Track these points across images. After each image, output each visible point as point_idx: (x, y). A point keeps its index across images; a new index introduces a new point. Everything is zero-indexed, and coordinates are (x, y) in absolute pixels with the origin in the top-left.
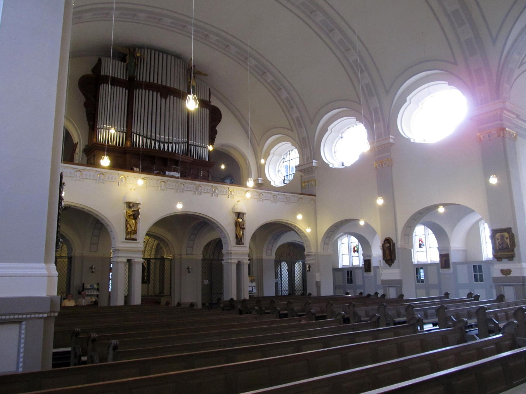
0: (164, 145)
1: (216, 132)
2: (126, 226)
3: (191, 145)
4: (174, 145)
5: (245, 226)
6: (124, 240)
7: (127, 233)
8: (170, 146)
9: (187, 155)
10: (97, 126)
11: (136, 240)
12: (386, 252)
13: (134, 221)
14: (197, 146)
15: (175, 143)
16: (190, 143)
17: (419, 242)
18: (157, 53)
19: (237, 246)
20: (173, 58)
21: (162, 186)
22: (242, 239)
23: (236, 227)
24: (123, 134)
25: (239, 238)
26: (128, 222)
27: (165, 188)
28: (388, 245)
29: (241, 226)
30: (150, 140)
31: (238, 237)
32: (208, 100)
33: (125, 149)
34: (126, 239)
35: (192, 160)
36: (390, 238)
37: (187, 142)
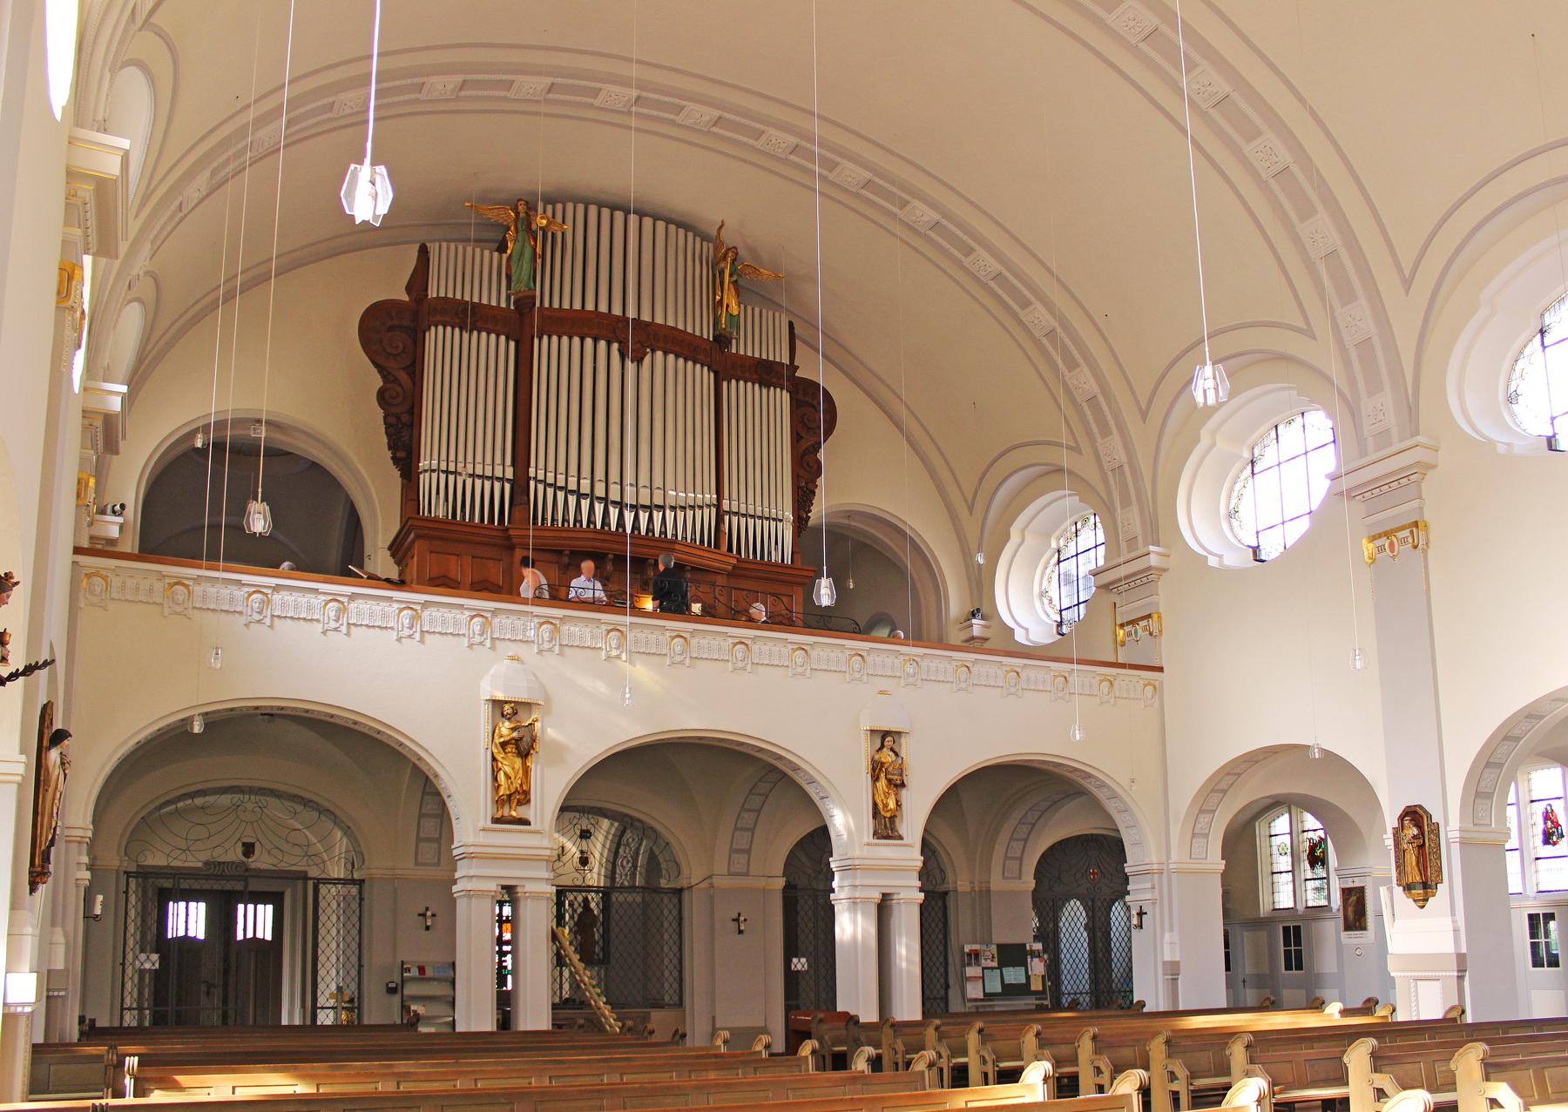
0: (636, 517)
2: (495, 779)
3: (729, 513)
4: (670, 515)
5: (905, 778)
6: (489, 825)
7: (500, 802)
8: (657, 516)
9: (717, 546)
10: (419, 462)
11: (526, 822)
12: (1407, 856)
13: (518, 762)
14: (752, 516)
15: (673, 508)
16: (726, 508)
17: (1545, 823)
18: (606, 212)
19: (877, 845)
20: (661, 225)
22: (897, 820)
23: (875, 779)
24: (503, 484)
25: (885, 818)
26: (500, 765)
28: (1415, 831)
29: (889, 776)
31: (882, 813)
33: (511, 532)
34: (496, 821)
35: (735, 561)
36: (1420, 807)
37: (715, 502)
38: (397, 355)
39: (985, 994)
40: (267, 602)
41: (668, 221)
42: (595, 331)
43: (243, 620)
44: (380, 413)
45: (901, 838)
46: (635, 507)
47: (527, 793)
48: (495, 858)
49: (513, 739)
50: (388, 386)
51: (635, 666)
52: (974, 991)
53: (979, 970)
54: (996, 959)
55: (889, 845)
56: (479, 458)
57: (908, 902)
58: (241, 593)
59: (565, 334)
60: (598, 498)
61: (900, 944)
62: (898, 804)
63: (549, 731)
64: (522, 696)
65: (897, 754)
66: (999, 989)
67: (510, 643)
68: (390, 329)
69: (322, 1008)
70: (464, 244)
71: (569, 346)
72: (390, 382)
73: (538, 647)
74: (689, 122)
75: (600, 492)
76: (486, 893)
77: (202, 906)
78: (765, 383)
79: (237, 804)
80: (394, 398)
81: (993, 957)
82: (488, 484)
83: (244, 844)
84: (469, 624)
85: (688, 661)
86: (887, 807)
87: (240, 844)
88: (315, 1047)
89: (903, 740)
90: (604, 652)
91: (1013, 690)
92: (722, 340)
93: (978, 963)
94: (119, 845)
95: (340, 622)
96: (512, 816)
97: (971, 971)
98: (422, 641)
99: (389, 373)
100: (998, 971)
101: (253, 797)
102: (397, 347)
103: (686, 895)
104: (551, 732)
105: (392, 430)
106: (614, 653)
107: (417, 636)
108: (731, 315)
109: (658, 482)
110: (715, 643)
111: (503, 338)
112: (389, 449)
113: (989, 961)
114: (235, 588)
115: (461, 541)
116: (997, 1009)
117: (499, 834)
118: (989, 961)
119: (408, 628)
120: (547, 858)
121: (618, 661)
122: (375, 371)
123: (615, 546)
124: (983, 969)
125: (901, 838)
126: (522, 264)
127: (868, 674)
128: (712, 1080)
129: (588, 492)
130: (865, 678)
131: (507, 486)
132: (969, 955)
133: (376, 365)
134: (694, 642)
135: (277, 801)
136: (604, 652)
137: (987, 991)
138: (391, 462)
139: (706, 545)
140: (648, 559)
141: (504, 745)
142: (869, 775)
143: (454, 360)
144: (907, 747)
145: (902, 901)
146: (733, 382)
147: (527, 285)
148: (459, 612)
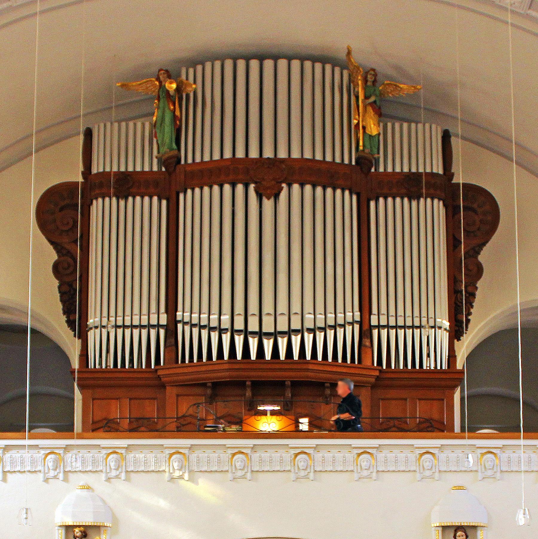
8: (296, 340)
10: (87, 321)
15: (312, 331)
42: (231, 177)
44: (56, 283)
46: (312, 331)
50: (62, 259)
56: (136, 310)
59: (207, 185)
64: (88, 520)
67: (81, 474)
68: (62, 209)
72: (63, 255)
75: (239, 324)
80: (66, 269)
82: (144, 332)
85: (311, 475)
90: (167, 475)
99: (63, 248)
107: (61, 476)
109: (296, 308)
111: (155, 199)
112: (64, 313)
115: (120, 386)
119: (115, 469)
121: (181, 482)
122: (51, 247)
127: (440, 471)
129: (242, 327)
130: (437, 475)
131: (162, 332)
136: (167, 475)
138: (66, 325)
139: (356, 363)
143: (153, 225)
147: (171, 149)
148: (96, 451)
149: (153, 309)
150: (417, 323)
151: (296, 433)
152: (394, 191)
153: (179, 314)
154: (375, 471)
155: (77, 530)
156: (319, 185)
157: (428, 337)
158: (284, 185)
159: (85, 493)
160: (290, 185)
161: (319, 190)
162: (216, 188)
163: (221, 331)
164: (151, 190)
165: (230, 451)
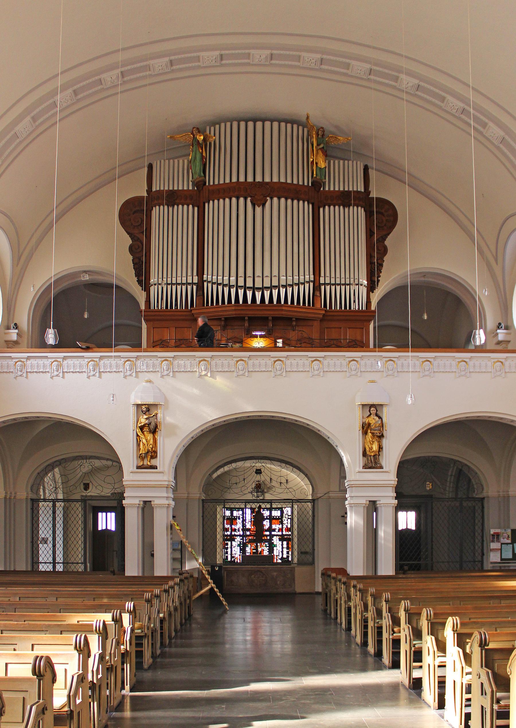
1: (384, 251)
3: (325, 284)
7: (141, 457)
8: (275, 292)
10: (150, 281)
11: (155, 467)
19: (364, 472)
21: (165, 369)
23: (365, 433)
25: (370, 456)
27: (170, 372)
30: (243, 290)
32: (361, 189)
33: (193, 312)
34: (138, 467)
35: (323, 312)
38: (139, 225)
39: (502, 559)
40: (24, 366)
41: (280, 121)
42: (236, 193)
43: (12, 375)
44: (131, 257)
45: (381, 467)
47: (155, 452)
48: (153, 487)
49: (146, 424)
51: (216, 379)
52: (494, 557)
53: (499, 544)
54: (510, 538)
55: (373, 472)
56: (179, 274)
57: (386, 505)
58: (12, 362)
60: (249, 288)
61: (381, 530)
62: (380, 448)
63: (167, 418)
64: (150, 401)
65: (380, 418)
66: (510, 556)
69: (50, 563)
70: (182, 158)
71: (223, 204)
73: (161, 374)
74: (256, 61)
75: (241, 283)
76: (133, 505)
77: (113, 514)
78: (346, 205)
79: (81, 464)
81: (508, 537)
82: (184, 287)
83: (84, 484)
84: (161, 365)
86: (371, 449)
87: (82, 484)
88: (47, 581)
89: (385, 409)
91: (463, 373)
92: (317, 184)
93: (498, 540)
94: (27, 485)
95: (59, 371)
96: (147, 464)
97: (494, 545)
98: (63, 377)
100: (511, 545)
101: (88, 460)
102: (138, 221)
103: (316, 502)
104: (169, 419)
105: (137, 266)
106: (204, 373)
107: (134, 374)
108: (320, 168)
109: (275, 272)
110: (263, 362)
111: (191, 206)
113: (505, 539)
114: (9, 360)
116: (511, 568)
117: (149, 474)
118: (505, 539)
120: (167, 486)
121: (206, 378)
123: (272, 313)
124: (502, 544)
125: (381, 467)
126: (196, 163)
127: (361, 371)
128: (104, 602)
129: (243, 284)
131: (195, 287)
132: (493, 535)
133: (128, 233)
134: (213, 363)
135: (98, 460)
137: (503, 557)
140: (268, 317)
141: (142, 428)
142: (361, 431)
144: (385, 413)
145: (382, 505)
146: (327, 207)
147: (200, 176)
149: (189, 273)
150: (348, 282)
151: (275, 348)
152: (335, 202)
153: (205, 276)
154: (322, 371)
155: (143, 407)
156: (289, 198)
157: (354, 290)
158: (268, 198)
159: (148, 384)
160: (272, 198)
161: (289, 201)
162: (227, 200)
163: (230, 287)
164: (188, 201)
165: (235, 359)
